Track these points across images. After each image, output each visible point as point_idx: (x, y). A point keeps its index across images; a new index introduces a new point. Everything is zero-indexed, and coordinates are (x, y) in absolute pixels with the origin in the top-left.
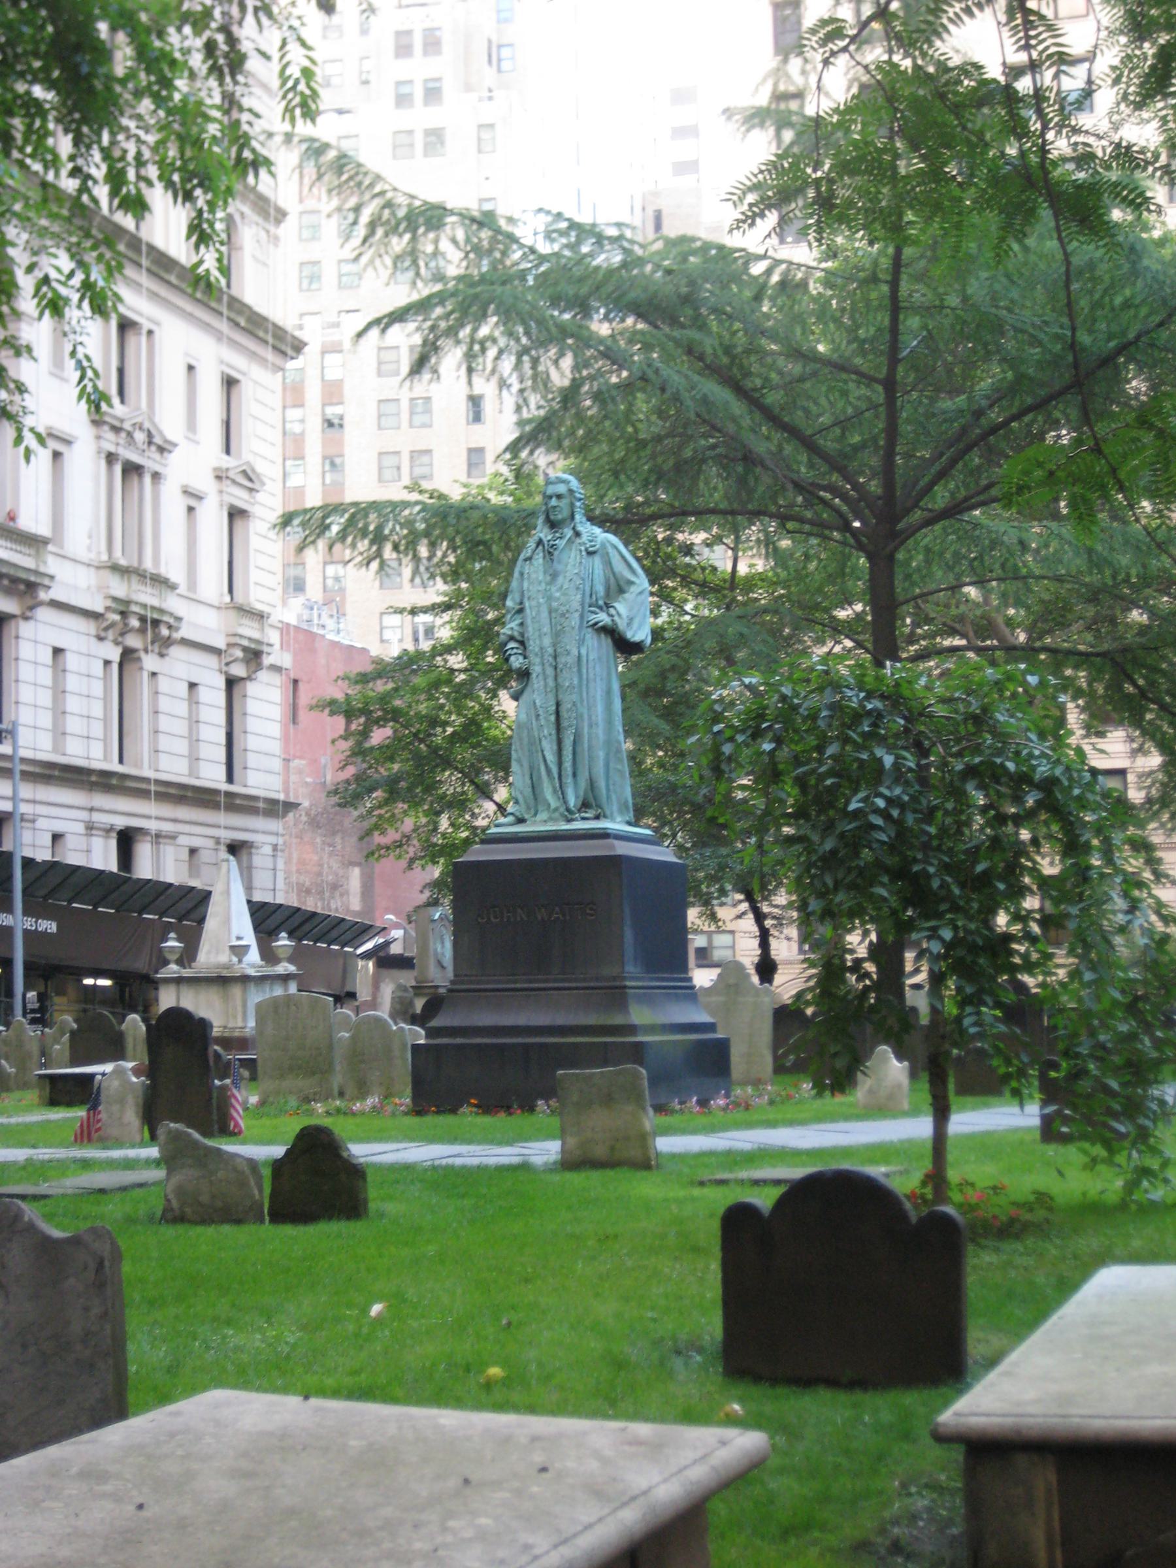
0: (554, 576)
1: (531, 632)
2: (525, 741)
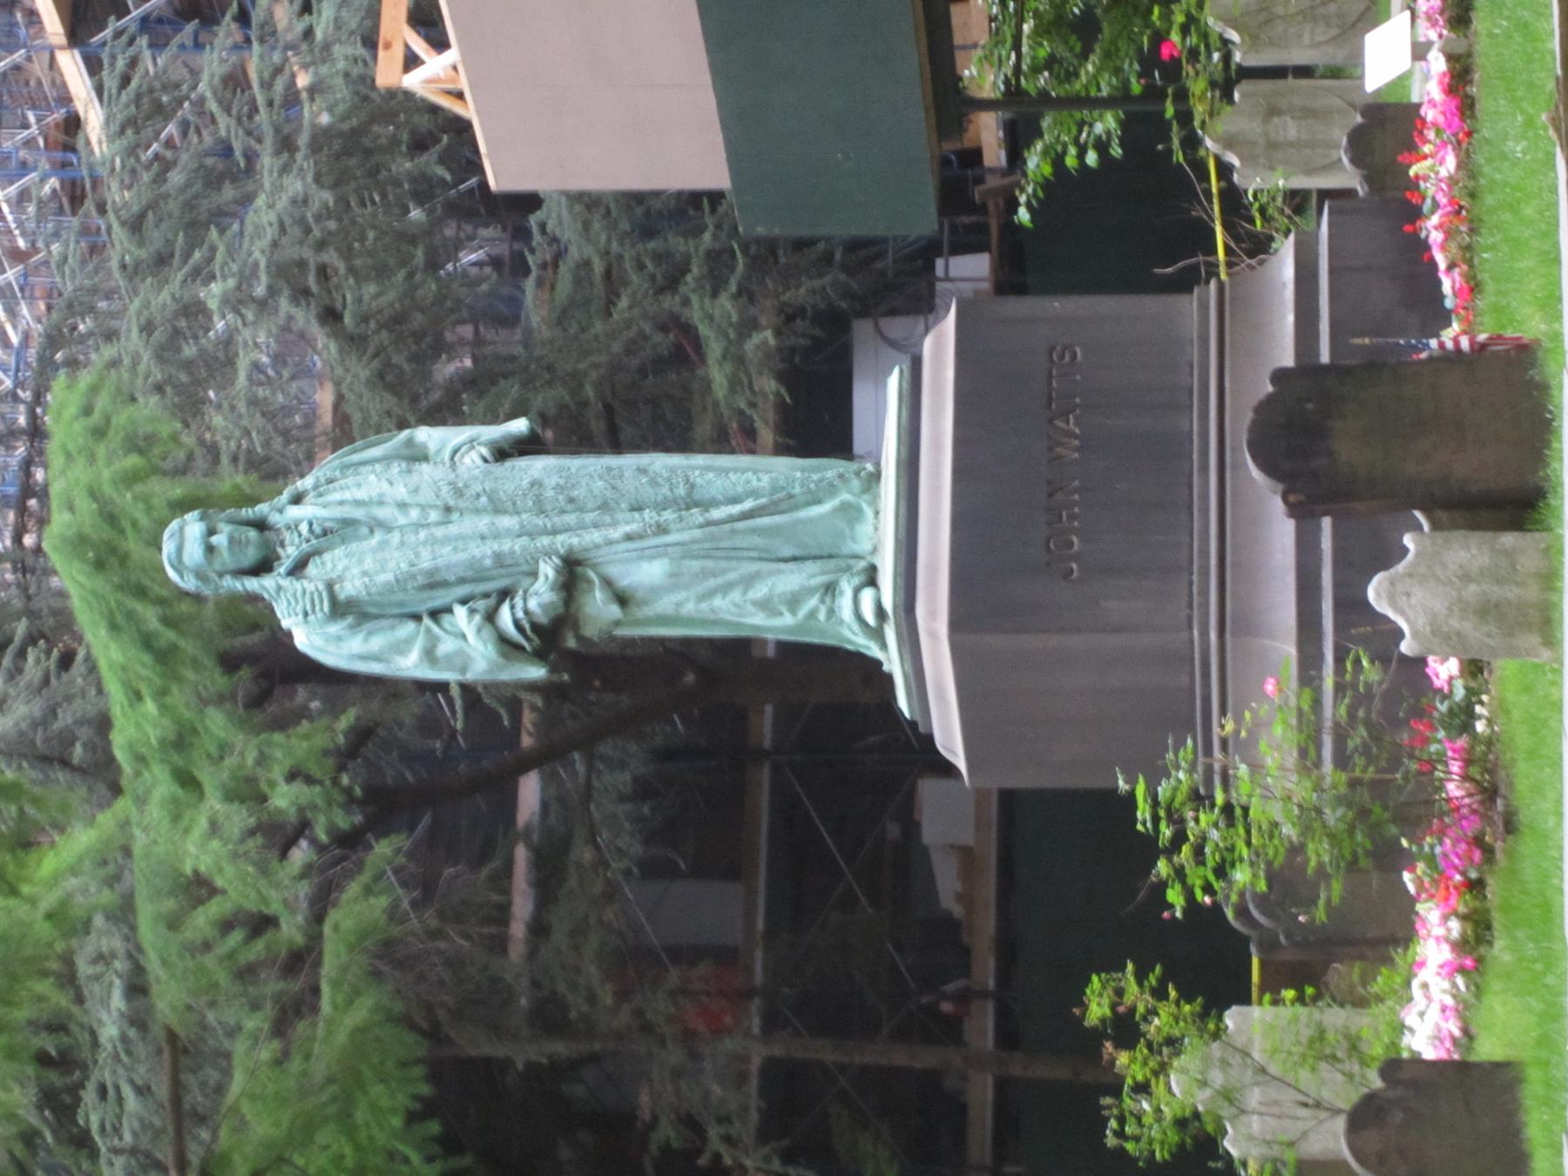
0: (375, 525)
1: (483, 552)
2: (709, 564)
